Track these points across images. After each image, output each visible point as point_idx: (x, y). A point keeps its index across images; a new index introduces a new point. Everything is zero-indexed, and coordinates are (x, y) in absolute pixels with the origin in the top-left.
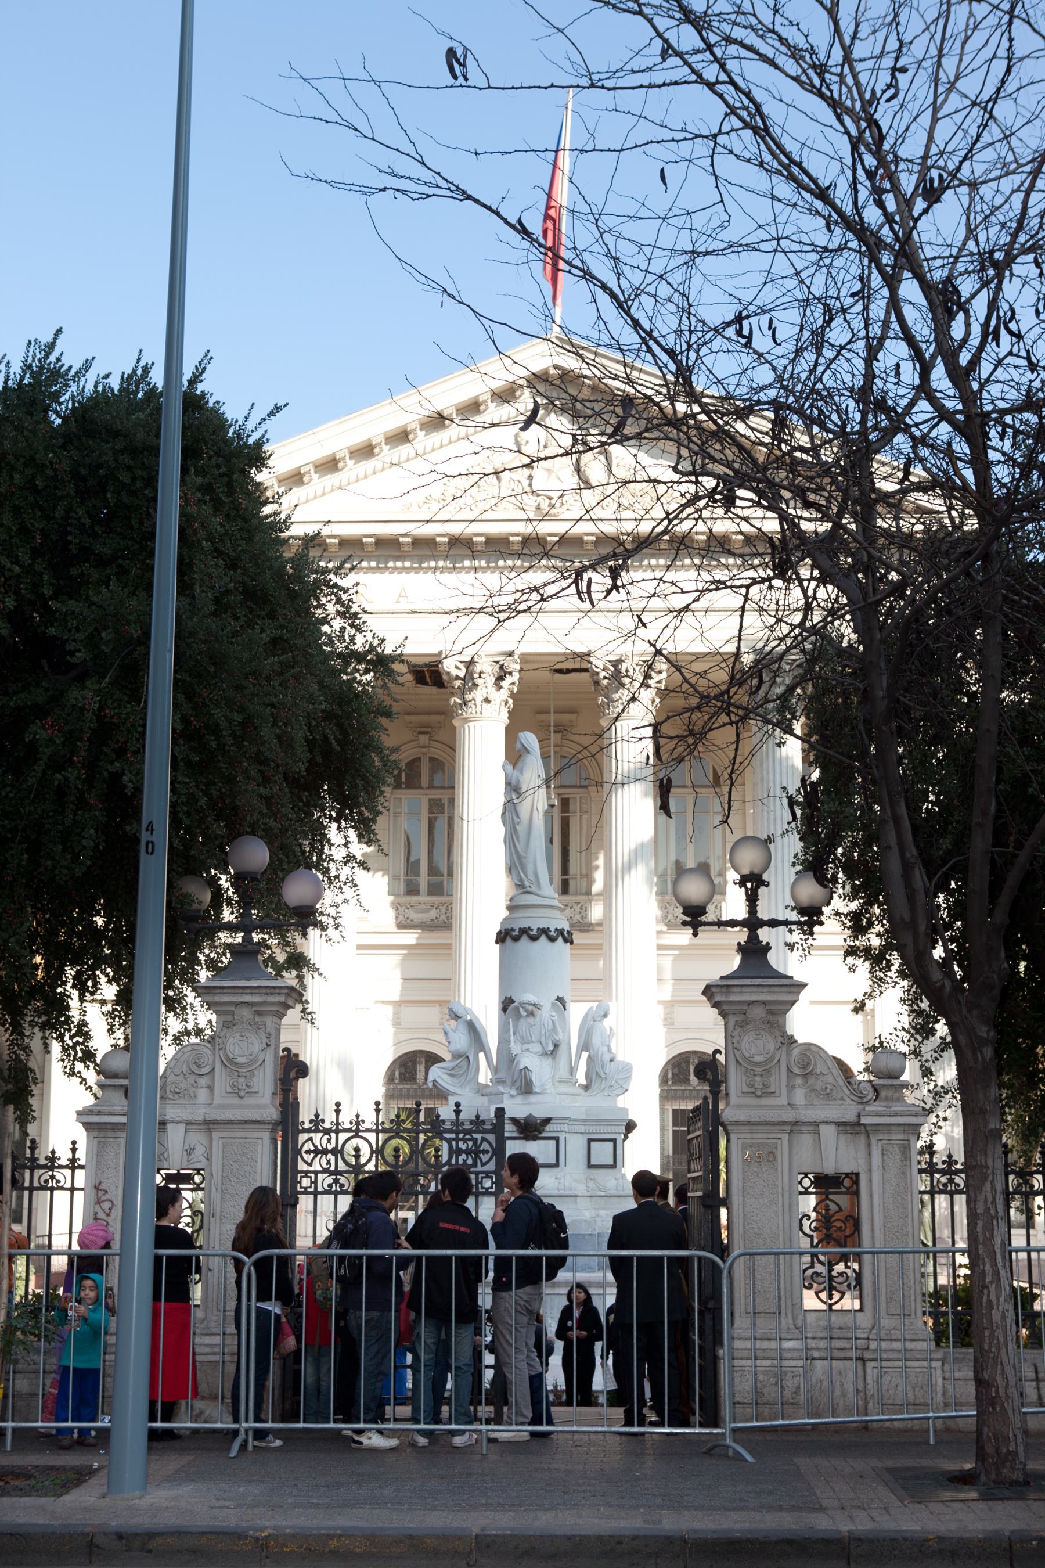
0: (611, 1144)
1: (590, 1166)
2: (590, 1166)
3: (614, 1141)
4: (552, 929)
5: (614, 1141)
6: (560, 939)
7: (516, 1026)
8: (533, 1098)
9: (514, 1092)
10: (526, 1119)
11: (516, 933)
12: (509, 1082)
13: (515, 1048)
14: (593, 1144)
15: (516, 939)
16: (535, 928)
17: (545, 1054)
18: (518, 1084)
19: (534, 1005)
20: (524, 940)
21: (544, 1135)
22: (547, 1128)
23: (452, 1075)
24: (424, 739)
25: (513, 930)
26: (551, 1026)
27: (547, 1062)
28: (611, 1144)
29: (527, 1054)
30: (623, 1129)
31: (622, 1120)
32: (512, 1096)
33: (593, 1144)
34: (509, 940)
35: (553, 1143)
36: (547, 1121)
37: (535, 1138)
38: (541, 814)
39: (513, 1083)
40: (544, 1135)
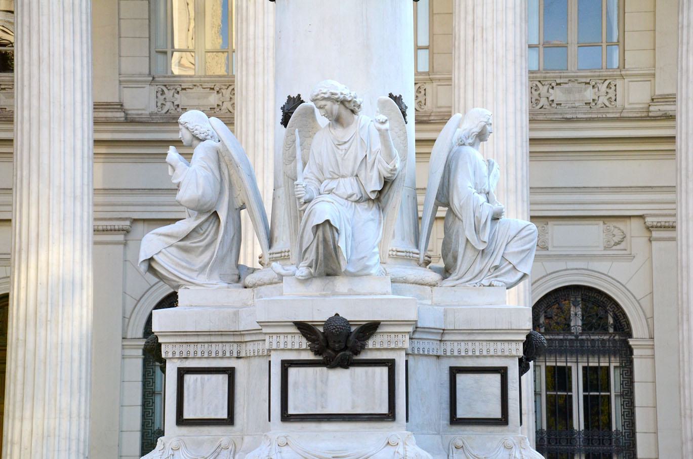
0: (497, 377)
1: (454, 420)
2: (454, 420)
3: (503, 372)
5: (503, 372)
7: (305, 147)
8: (341, 284)
10: (328, 323)
12: (294, 256)
14: (461, 378)
17: (364, 199)
18: (311, 256)
19: (343, 102)
21: (365, 356)
22: (370, 344)
23: (179, 247)
27: (367, 213)
28: (497, 377)
31: (518, 331)
33: (461, 378)
36: (371, 328)
37: (346, 364)
39: (303, 254)
40: (364, 356)
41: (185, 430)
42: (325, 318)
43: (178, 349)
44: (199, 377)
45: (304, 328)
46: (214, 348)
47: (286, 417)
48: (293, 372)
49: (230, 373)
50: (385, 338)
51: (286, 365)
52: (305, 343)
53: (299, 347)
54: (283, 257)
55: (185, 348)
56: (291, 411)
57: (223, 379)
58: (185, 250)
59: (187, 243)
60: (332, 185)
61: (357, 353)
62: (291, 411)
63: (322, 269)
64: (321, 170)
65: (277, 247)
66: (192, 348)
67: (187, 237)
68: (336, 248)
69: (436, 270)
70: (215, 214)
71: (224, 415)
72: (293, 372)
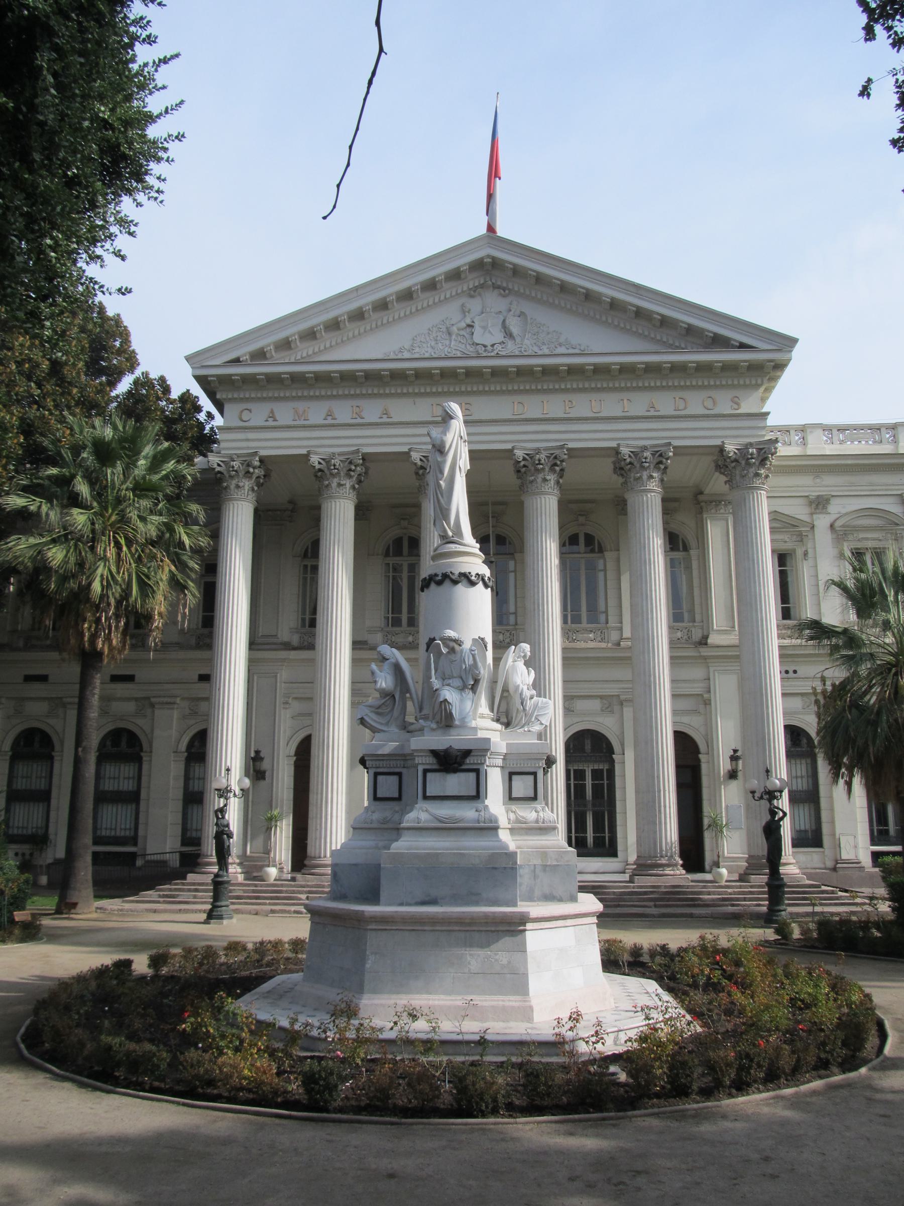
1: (511, 798)
3: (535, 774)
4: (473, 574)
6: (481, 584)
8: (453, 731)
9: (434, 726)
11: (440, 578)
12: (431, 716)
13: (436, 683)
15: (439, 583)
16: (457, 573)
18: (438, 717)
20: (447, 583)
21: (464, 767)
24: (404, 523)
25: (436, 575)
26: (471, 662)
29: (447, 688)
30: (543, 764)
32: (433, 730)
34: (433, 586)
35: (472, 776)
36: (467, 753)
37: (455, 771)
38: (464, 475)
39: (434, 718)
40: (464, 767)
41: (377, 803)
42: (444, 747)
43: (374, 763)
44: (384, 777)
45: (434, 753)
46: (392, 763)
47: (425, 797)
48: (429, 775)
49: (400, 775)
50: (475, 758)
51: (425, 771)
52: (435, 761)
53: (430, 761)
54: (426, 718)
55: (377, 763)
56: (428, 794)
57: (395, 779)
58: (378, 714)
59: (380, 710)
60: (451, 681)
61: (461, 765)
62: (428, 794)
63: (443, 723)
64: (444, 674)
65: (425, 712)
66: (381, 763)
67: (379, 707)
68: (451, 714)
69: (502, 724)
70: (393, 696)
71: (396, 795)
72: (429, 775)
